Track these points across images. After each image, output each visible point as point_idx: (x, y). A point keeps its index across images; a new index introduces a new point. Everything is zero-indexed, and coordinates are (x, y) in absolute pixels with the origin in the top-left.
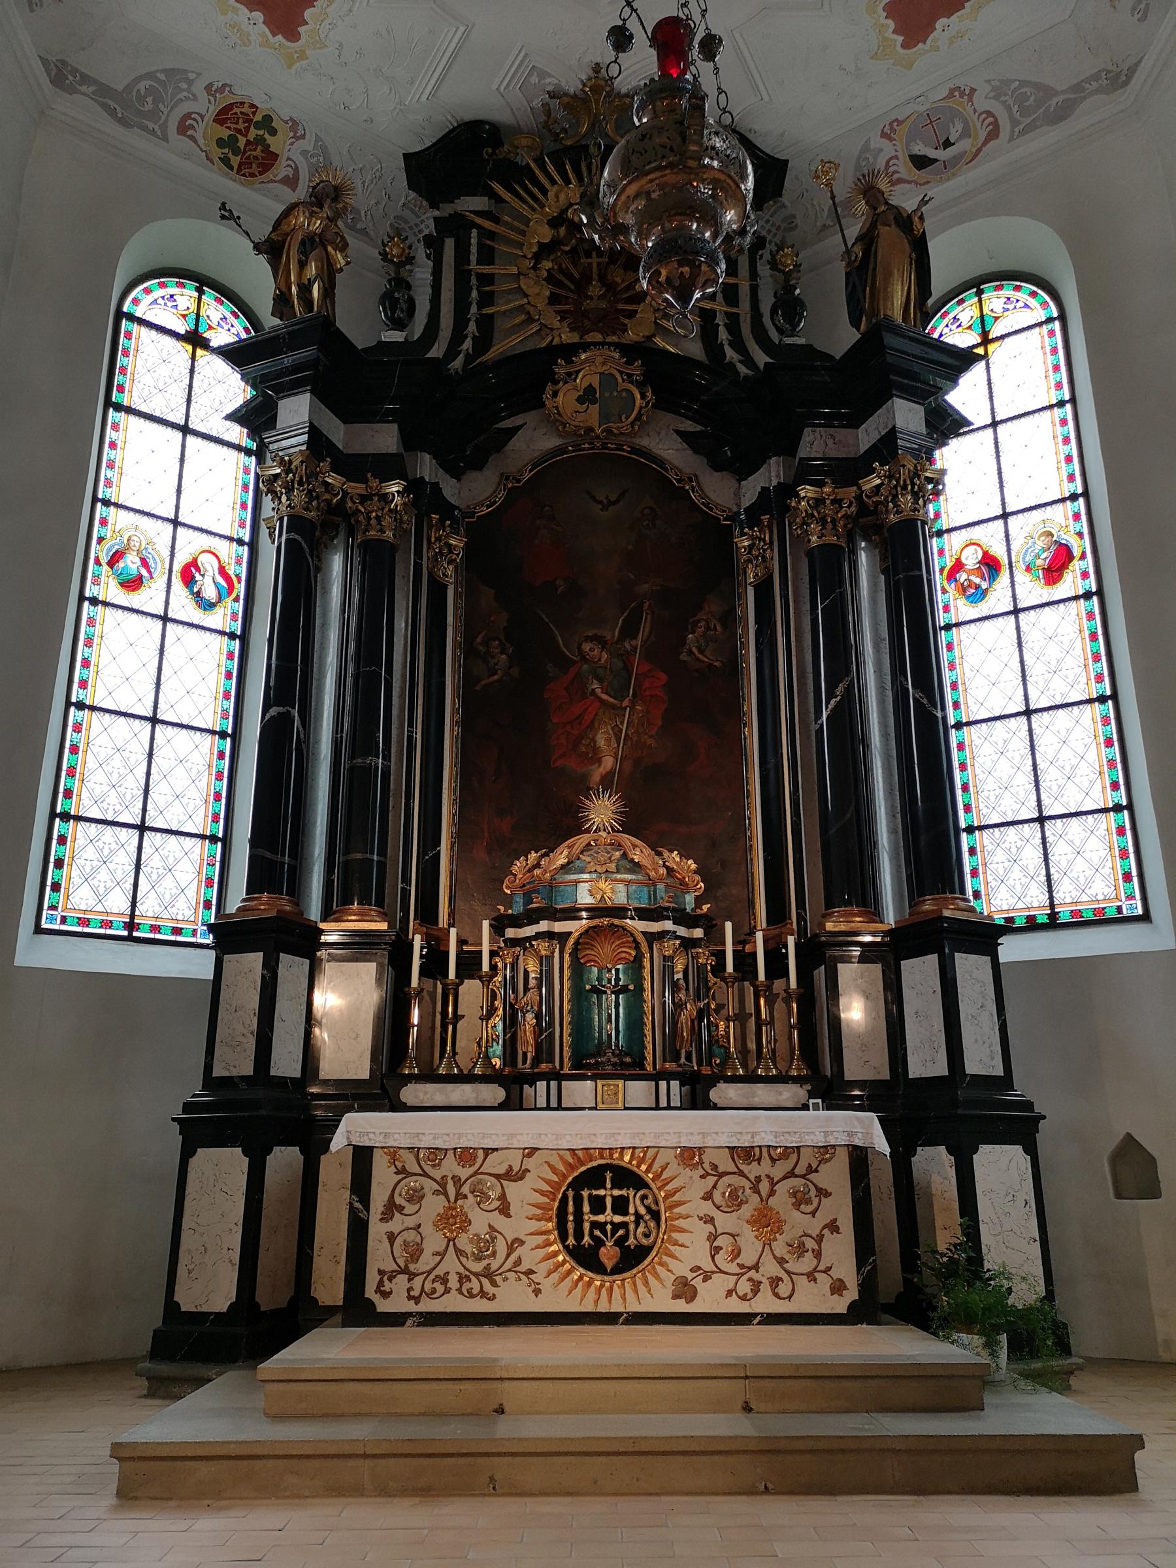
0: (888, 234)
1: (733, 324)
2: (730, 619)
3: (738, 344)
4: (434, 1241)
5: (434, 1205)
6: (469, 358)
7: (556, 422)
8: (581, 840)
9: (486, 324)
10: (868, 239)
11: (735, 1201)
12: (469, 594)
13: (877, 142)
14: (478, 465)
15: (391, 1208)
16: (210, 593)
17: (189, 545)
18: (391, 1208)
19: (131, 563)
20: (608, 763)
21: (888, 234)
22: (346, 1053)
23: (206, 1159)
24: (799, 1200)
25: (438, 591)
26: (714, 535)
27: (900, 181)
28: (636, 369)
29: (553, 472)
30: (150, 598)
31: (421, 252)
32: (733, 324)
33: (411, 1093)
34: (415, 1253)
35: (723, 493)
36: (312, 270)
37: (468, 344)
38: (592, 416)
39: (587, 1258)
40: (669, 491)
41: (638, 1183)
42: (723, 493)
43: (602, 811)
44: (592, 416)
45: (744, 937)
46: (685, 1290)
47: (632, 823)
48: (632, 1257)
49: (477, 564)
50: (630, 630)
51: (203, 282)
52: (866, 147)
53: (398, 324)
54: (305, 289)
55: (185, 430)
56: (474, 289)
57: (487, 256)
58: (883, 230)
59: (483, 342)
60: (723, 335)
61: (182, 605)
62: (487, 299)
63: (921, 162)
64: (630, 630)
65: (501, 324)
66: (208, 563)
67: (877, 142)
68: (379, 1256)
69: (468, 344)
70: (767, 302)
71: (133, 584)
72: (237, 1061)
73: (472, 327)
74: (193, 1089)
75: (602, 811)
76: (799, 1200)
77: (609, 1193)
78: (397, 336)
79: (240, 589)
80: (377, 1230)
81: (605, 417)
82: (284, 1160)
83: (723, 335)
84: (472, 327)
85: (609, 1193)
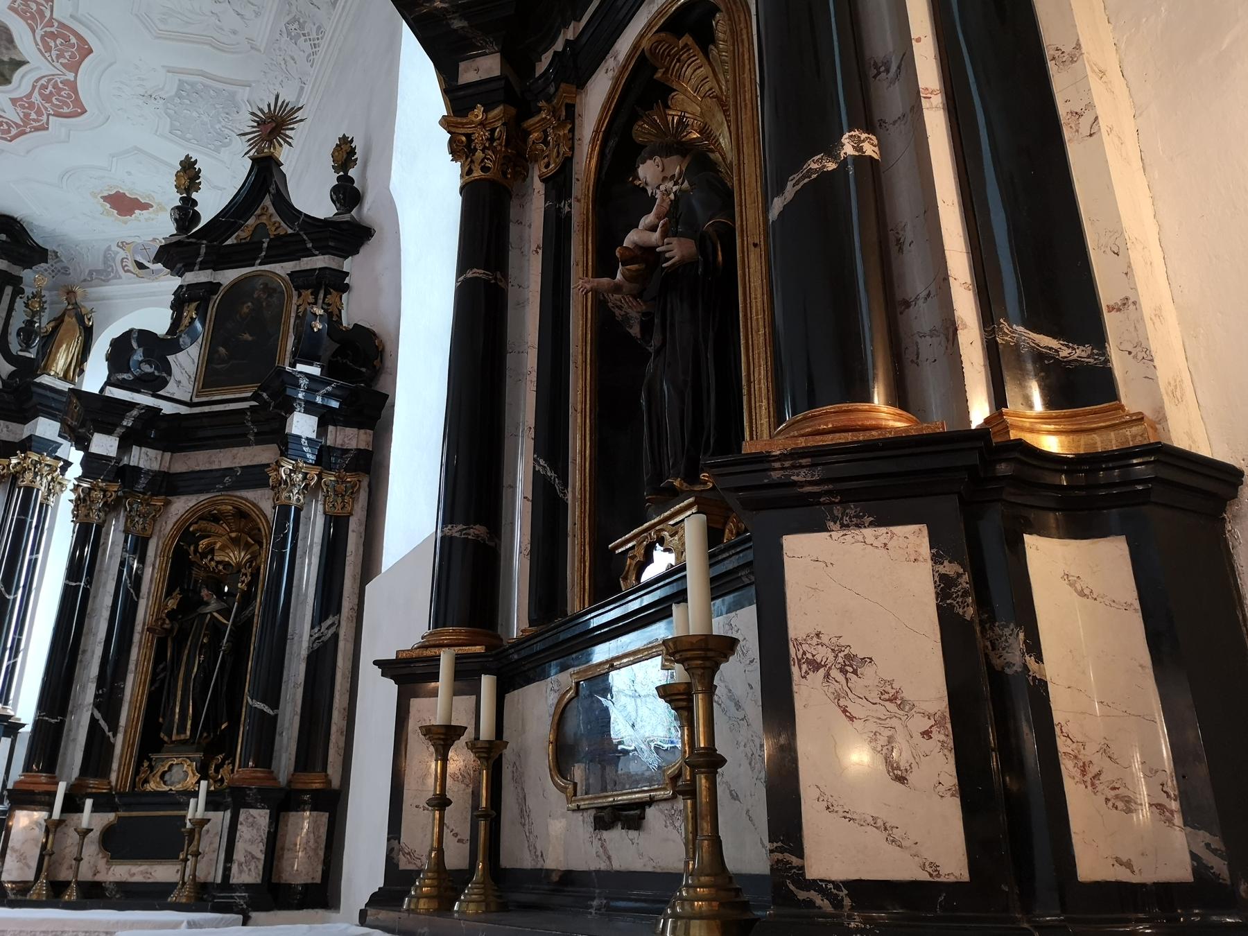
0: (70, 321)
10: (59, 321)
13: (114, 248)
21: (70, 321)
27: (128, 271)
52: (109, 248)
58: (67, 319)
63: (141, 266)
67: (114, 248)
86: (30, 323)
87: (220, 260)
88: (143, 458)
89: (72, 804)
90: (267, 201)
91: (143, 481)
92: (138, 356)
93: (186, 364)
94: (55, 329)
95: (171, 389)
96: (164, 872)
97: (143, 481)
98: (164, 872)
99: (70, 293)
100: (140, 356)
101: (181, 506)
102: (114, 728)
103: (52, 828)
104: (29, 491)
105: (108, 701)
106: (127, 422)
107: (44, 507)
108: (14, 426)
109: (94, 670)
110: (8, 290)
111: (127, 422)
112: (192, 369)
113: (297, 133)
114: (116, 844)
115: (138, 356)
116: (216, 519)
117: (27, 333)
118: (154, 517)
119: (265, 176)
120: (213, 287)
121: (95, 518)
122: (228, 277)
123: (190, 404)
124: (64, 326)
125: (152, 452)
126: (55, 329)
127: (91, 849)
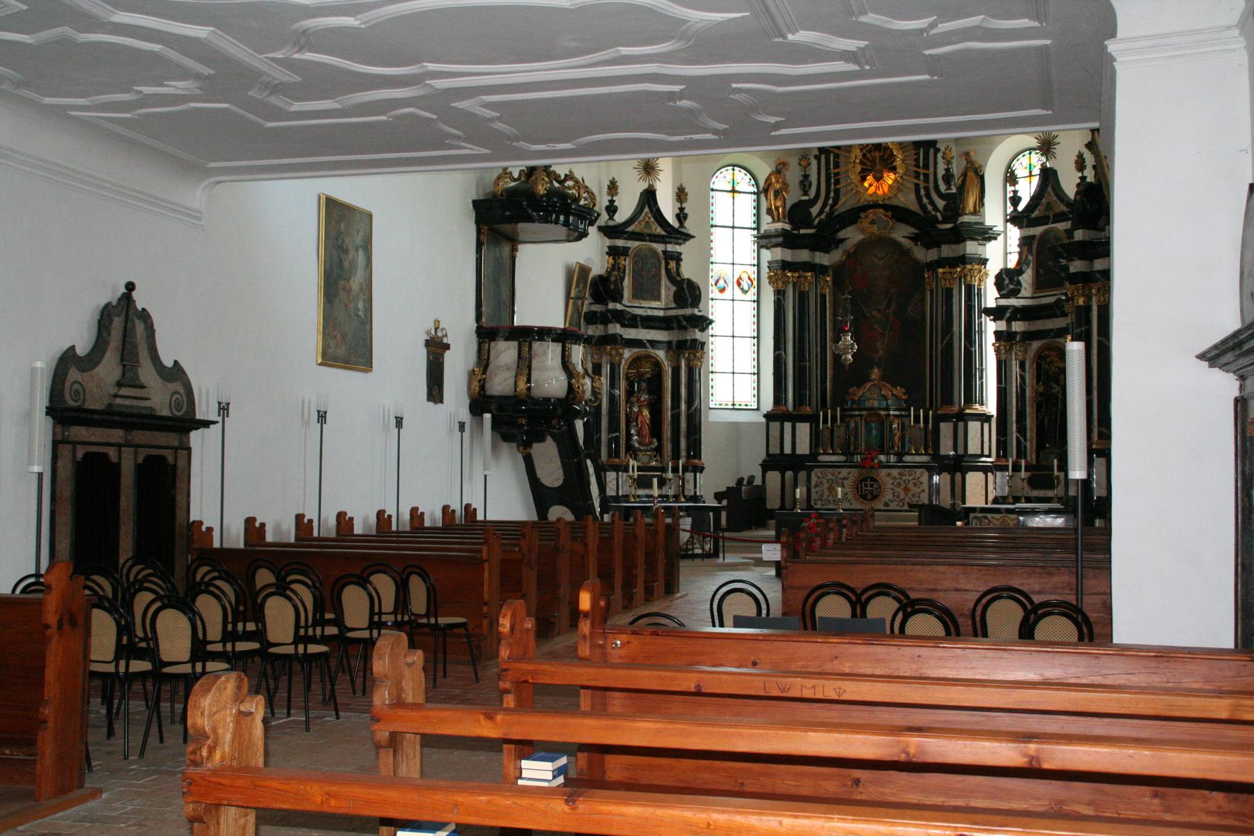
0: (971, 174)
1: (927, 189)
2: (923, 300)
3: (928, 196)
4: (826, 493)
5: (827, 485)
6: (832, 207)
7: (863, 231)
8: (868, 385)
9: (837, 192)
10: (964, 175)
11: (899, 485)
12: (834, 294)
14: (837, 247)
15: (816, 486)
16: (746, 288)
17: (739, 271)
18: (816, 486)
19: (721, 283)
20: (881, 352)
21: (971, 174)
22: (803, 448)
23: (770, 474)
24: (915, 485)
25: (823, 297)
26: (919, 269)
28: (889, 214)
29: (861, 246)
30: (728, 294)
31: (814, 163)
32: (927, 189)
33: (822, 458)
34: (822, 495)
35: (922, 254)
36: (779, 203)
37: (830, 202)
38: (874, 229)
39: (864, 497)
40: (905, 253)
41: (875, 480)
42: (922, 254)
43: (876, 373)
44: (874, 229)
45: (917, 411)
46: (886, 504)
47: (883, 378)
48: (874, 497)
49: (838, 285)
50: (888, 307)
51: (734, 166)
53: (806, 193)
54: (777, 208)
55: (733, 227)
56: (833, 180)
57: (837, 165)
59: (836, 201)
60: (922, 192)
61: (738, 294)
62: (837, 182)
64: (888, 307)
65: (842, 191)
66: (745, 277)
68: (814, 496)
69: (830, 202)
70: (941, 172)
71: (722, 290)
72: (775, 450)
73: (832, 194)
74: (763, 456)
75: (876, 373)
76: (915, 485)
77: (869, 483)
78: (806, 198)
79: (755, 283)
80: (813, 490)
81: (879, 228)
82: (789, 474)
83: (922, 192)
84: (832, 194)
85: (869, 483)
86: (947, 170)
87: (1034, 223)
88: (1018, 326)
89: (1016, 468)
90: (1050, 189)
91: (1018, 338)
92: (1007, 282)
93: (1027, 279)
94: (964, 182)
95: (1023, 293)
96: (1050, 493)
97: (1018, 338)
98: (1050, 493)
99: (967, 154)
100: (1007, 281)
101: (1036, 345)
102: (1025, 440)
103: (1011, 477)
104: (969, 288)
105: (1022, 430)
106: (1008, 315)
107: (979, 290)
108: (954, 246)
109: (1014, 418)
110: (932, 151)
111: (1008, 315)
112: (1030, 281)
113: (1058, 150)
114: (1033, 483)
115: (1007, 282)
116: (1051, 350)
117: (948, 177)
118: (1025, 352)
119: (1048, 176)
120: (1033, 237)
121: (1003, 357)
122: (1038, 231)
123: (1032, 298)
124: (968, 180)
125: (1020, 323)
126: (964, 182)
127: (1025, 484)
